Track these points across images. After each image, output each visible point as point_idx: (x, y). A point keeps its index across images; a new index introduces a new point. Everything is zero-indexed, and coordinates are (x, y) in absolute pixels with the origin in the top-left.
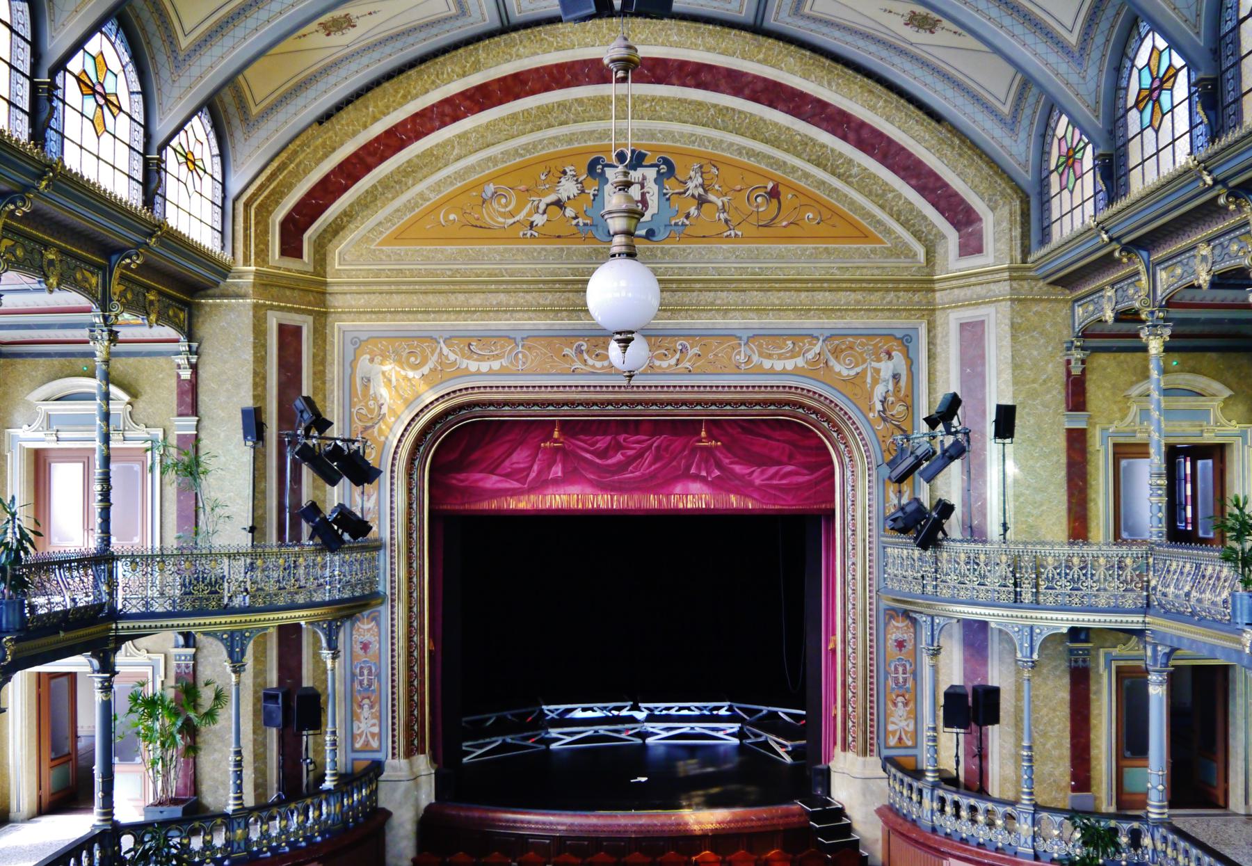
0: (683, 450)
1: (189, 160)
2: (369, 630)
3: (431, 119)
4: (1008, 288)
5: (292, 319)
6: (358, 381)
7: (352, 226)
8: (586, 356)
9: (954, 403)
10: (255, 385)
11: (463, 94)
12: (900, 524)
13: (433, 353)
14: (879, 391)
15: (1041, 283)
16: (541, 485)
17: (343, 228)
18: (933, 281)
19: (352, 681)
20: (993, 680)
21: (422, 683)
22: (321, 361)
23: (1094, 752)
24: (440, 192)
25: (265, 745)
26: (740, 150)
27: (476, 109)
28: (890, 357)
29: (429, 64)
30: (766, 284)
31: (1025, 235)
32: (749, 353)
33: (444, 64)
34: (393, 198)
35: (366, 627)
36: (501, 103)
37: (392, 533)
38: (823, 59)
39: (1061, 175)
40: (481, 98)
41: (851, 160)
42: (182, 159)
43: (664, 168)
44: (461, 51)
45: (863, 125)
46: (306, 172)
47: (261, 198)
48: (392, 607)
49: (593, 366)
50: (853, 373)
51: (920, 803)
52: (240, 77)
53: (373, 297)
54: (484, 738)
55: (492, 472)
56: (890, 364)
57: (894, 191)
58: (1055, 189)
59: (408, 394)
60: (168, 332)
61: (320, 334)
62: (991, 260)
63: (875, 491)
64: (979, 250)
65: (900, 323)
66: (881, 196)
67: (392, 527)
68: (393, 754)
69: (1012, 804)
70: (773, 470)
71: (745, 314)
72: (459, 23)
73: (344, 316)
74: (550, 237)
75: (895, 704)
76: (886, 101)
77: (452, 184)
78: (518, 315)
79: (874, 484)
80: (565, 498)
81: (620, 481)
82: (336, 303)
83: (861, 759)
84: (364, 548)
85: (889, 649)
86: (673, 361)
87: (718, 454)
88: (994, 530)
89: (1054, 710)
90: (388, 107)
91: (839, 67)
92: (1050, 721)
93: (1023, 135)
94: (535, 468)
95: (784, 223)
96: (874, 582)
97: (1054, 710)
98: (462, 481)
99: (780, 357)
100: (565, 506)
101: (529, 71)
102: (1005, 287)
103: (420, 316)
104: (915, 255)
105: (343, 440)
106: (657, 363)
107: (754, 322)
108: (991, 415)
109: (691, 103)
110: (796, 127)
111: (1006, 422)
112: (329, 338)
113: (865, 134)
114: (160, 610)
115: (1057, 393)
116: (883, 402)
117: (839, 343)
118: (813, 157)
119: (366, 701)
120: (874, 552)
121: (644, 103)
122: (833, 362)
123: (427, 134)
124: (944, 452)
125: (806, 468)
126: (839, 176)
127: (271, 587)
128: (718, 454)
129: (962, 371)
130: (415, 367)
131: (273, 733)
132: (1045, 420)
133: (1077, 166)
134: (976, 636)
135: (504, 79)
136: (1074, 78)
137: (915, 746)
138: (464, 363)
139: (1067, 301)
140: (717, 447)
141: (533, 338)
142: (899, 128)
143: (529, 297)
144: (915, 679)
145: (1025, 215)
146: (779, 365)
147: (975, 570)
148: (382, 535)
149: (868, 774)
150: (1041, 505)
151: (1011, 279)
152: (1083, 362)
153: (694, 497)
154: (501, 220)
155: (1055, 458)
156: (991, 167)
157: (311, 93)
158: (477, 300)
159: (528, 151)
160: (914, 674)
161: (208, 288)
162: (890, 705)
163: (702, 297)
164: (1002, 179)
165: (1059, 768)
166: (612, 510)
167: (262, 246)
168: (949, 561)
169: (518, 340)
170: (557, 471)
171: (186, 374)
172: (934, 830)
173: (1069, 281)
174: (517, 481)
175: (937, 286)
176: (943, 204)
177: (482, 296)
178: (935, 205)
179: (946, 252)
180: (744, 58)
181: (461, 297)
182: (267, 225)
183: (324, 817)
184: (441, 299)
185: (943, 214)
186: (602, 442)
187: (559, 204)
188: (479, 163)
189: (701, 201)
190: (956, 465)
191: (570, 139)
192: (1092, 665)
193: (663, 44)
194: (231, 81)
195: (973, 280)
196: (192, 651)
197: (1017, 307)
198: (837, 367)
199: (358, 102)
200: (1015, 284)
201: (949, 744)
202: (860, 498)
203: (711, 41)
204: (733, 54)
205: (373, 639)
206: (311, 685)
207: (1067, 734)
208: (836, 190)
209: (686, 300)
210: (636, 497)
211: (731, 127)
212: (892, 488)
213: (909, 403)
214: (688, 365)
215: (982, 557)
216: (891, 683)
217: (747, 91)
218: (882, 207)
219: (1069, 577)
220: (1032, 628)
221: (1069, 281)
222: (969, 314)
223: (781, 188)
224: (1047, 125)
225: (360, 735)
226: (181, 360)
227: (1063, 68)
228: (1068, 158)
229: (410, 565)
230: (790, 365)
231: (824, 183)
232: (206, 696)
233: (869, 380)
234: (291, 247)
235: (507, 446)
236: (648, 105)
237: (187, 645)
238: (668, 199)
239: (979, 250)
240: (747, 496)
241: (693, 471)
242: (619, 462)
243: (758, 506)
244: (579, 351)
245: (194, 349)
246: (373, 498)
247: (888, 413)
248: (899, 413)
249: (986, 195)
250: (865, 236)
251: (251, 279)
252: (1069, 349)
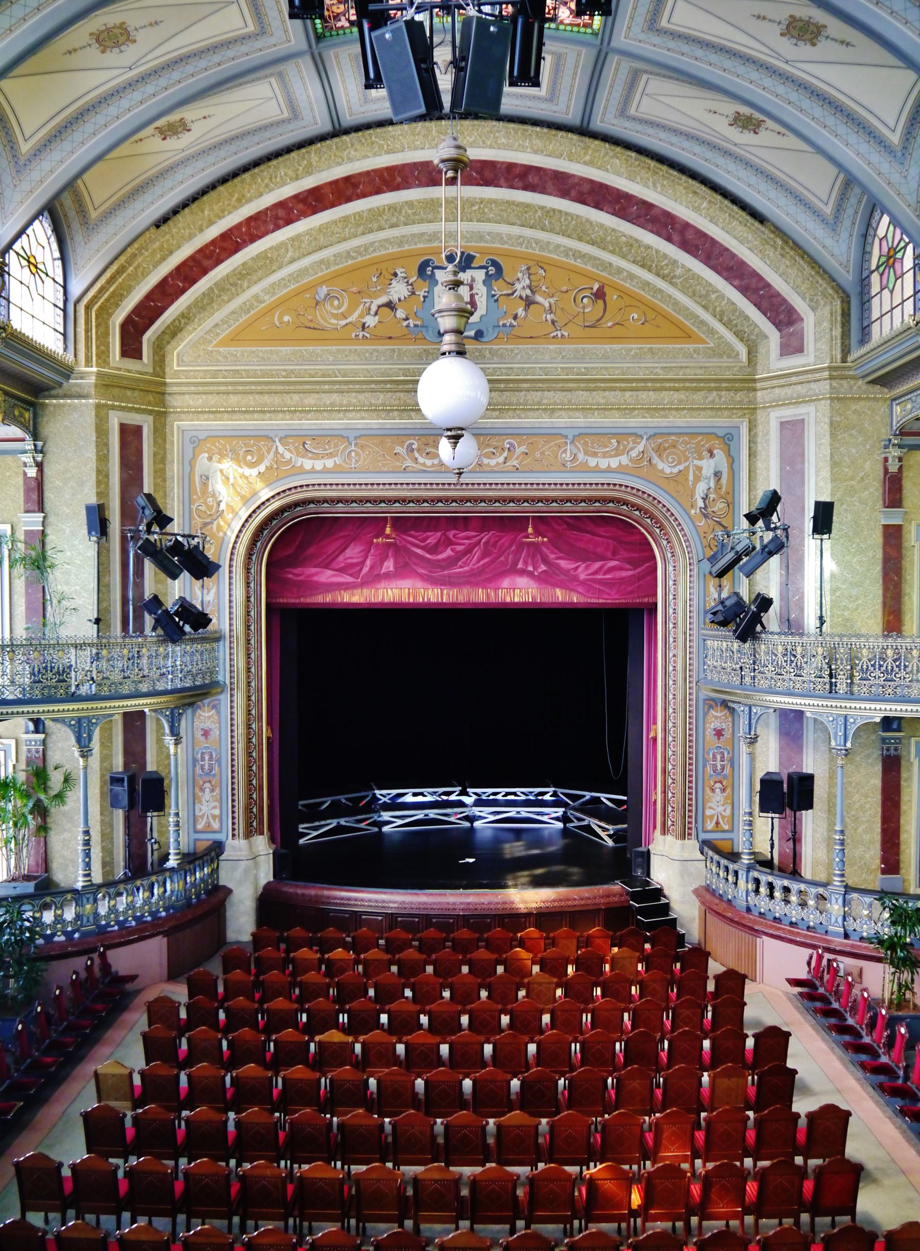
0: (511, 546)
1: (31, 263)
2: (209, 717)
3: (265, 222)
4: (828, 387)
5: (133, 419)
6: (197, 479)
7: (190, 328)
8: (417, 455)
9: (774, 499)
10: (99, 483)
11: (296, 197)
12: (720, 618)
13: (269, 452)
15: (860, 382)
16: (374, 578)
17: (181, 330)
18: (754, 381)
19: (194, 766)
20: (808, 769)
21: (260, 768)
22: (161, 459)
23: (903, 837)
24: (274, 294)
25: (111, 826)
26: (567, 252)
27: (309, 211)
28: (712, 455)
29: (262, 167)
30: (591, 384)
31: (846, 335)
32: (575, 451)
33: (277, 168)
34: (229, 301)
35: (207, 715)
36: (333, 206)
37: (231, 625)
38: (648, 161)
39: (881, 275)
40: (314, 201)
41: (675, 261)
42: (25, 263)
43: (492, 270)
44: (294, 154)
45: (687, 225)
46: (145, 274)
47: (101, 301)
48: (232, 695)
50: (675, 470)
51: (736, 884)
52: (79, 182)
53: (210, 397)
54: (319, 820)
55: (327, 567)
56: (712, 462)
57: (717, 291)
58: (875, 288)
59: (246, 491)
60: (14, 431)
61: (160, 432)
62: (811, 359)
63: (695, 585)
64: (800, 350)
65: (721, 422)
66: (705, 297)
67: (230, 619)
68: (233, 835)
69: (825, 885)
70: (597, 565)
71: (571, 413)
72: (291, 126)
73: (183, 416)
74: (381, 338)
75: (713, 790)
76: (710, 202)
77: (285, 286)
78: (351, 415)
79: (695, 579)
80: (396, 591)
81: (449, 576)
82: (176, 402)
83: (679, 842)
84: (204, 640)
85: (708, 738)
87: (545, 550)
88: (811, 622)
89: (866, 797)
90: (223, 211)
91: (665, 168)
92: (861, 807)
93: (844, 235)
94: (368, 562)
95: (610, 324)
96: (694, 674)
97: (866, 797)
98: (298, 575)
99: (605, 455)
100: (397, 600)
101: (360, 174)
102: (824, 387)
103: (256, 416)
104: (738, 354)
105: (183, 536)
106: (486, 461)
107: (580, 421)
108: (810, 512)
109: (519, 205)
110: (621, 229)
111: (824, 518)
112: (169, 437)
113: (690, 235)
114: (11, 697)
115: (875, 490)
116: (704, 499)
117: (663, 442)
118: (639, 258)
119: (207, 785)
120: (695, 644)
121: (473, 205)
123: (260, 237)
124: (764, 547)
125: (628, 563)
126: (664, 277)
127: (116, 676)
128: (545, 550)
129: (782, 469)
130: (252, 465)
131: (119, 814)
132: (861, 517)
133: (898, 265)
134: (792, 724)
135: (335, 183)
136: (896, 178)
137: (732, 831)
138: (300, 461)
139: (886, 400)
140: (543, 543)
141: (365, 436)
142: (723, 229)
143: (361, 397)
144: (732, 766)
145: (846, 314)
146: (604, 463)
147: (792, 661)
148: (222, 627)
149: (686, 856)
150: (857, 600)
151: (831, 378)
152: (900, 459)
153: (520, 591)
154: (334, 321)
155: (871, 554)
156: (813, 268)
157: (148, 197)
158: (311, 400)
159: (360, 254)
160: (732, 761)
161: (49, 389)
162: (708, 791)
163: (529, 397)
164: (823, 279)
165: (870, 851)
166: (442, 604)
167: (102, 348)
168: (767, 653)
169: (351, 439)
170: (389, 565)
171: (32, 472)
172: (749, 910)
173: (886, 380)
174: (351, 575)
175: (758, 385)
176: (765, 304)
177: (316, 396)
178: (758, 306)
179: (768, 352)
180: (571, 160)
181: (296, 397)
182: (107, 327)
183: (168, 893)
184: (277, 399)
185: (765, 314)
186: (433, 538)
187: (390, 305)
188: (312, 265)
189: (529, 302)
190: (775, 560)
191: (401, 241)
192: (904, 753)
193: (491, 147)
194: (70, 185)
195: (794, 379)
196: (42, 736)
197: (837, 405)
198: (660, 465)
199: (194, 206)
200: (834, 384)
201: (764, 828)
202: (682, 593)
203: (538, 143)
204: (560, 156)
205: (213, 726)
206: (154, 769)
207: (878, 820)
208: (661, 291)
209: (514, 400)
210: (465, 591)
211: (558, 229)
212: (712, 583)
213: (730, 500)
214: (515, 463)
215: (799, 649)
216: (709, 770)
217: (573, 193)
218: (705, 307)
219: (883, 669)
220: (846, 717)
221: (886, 380)
222: (788, 413)
223: (606, 289)
224: (869, 225)
226: (28, 458)
227: (885, 167)
228: (889, 258)
229: (248, 656)
230: (614, 463)
231: (649, 284)
232: (56, 780)
233: (691, 477)
234: (131, 349)
235: (340, 542)
236: (477, 207)
237: (37, 731)
238: (496, 301)
239: (800, 350)
240: (571, 590)
241: (520, 566)
242: (449, 558)
243: (582, 600)
244: (410, 450)
245: (39, 448)
246: (213, 592)
247: (710, 510)
248: (720, 509)
249: (807, 295)
250: (688, 336)
251: (92, 380)
252: (886, 447)
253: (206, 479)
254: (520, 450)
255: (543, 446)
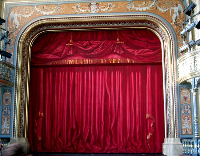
2: (8, 95)
6: (10, 19)
8: (79, 9)
13: (32, 10)
14: (174, 16)
28: (177, 6)
32: (131, 6)
35: (7, 94)
37: (17, 64)
49: (82, 12)
50: (165, 11)
56: (177, 8)
68: (14, 136)
85: (181, 100)
86: (107, 9)
99: (141, 7)
106: (102, 10)
112: (2, 7)
116: (176, 19)
119: (6, 118)
122: (158, 8)
128: (123, 46)
137: (192, 134)
144: (191, 110)
146: (141, 9)
149: (175, 143)
162: (183, 120)
198: (160, 9)
205: (9, 98)
214: (112, 10)
225: (4, 129)
230: (144, 9)
233: (171, 13)
247: (178, 23)
253: (13, 19)
254: (112, 6)
255: (121, 4)
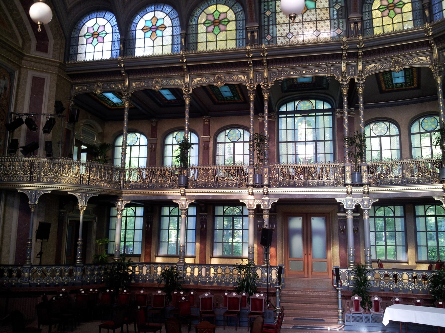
18: (24, 55)
28: (4, 79)
57: (18, 11)
62: (51, 56)
173: (73, 76)
175: (25, 58)
179: (30, 46)
222: (37, 74)
